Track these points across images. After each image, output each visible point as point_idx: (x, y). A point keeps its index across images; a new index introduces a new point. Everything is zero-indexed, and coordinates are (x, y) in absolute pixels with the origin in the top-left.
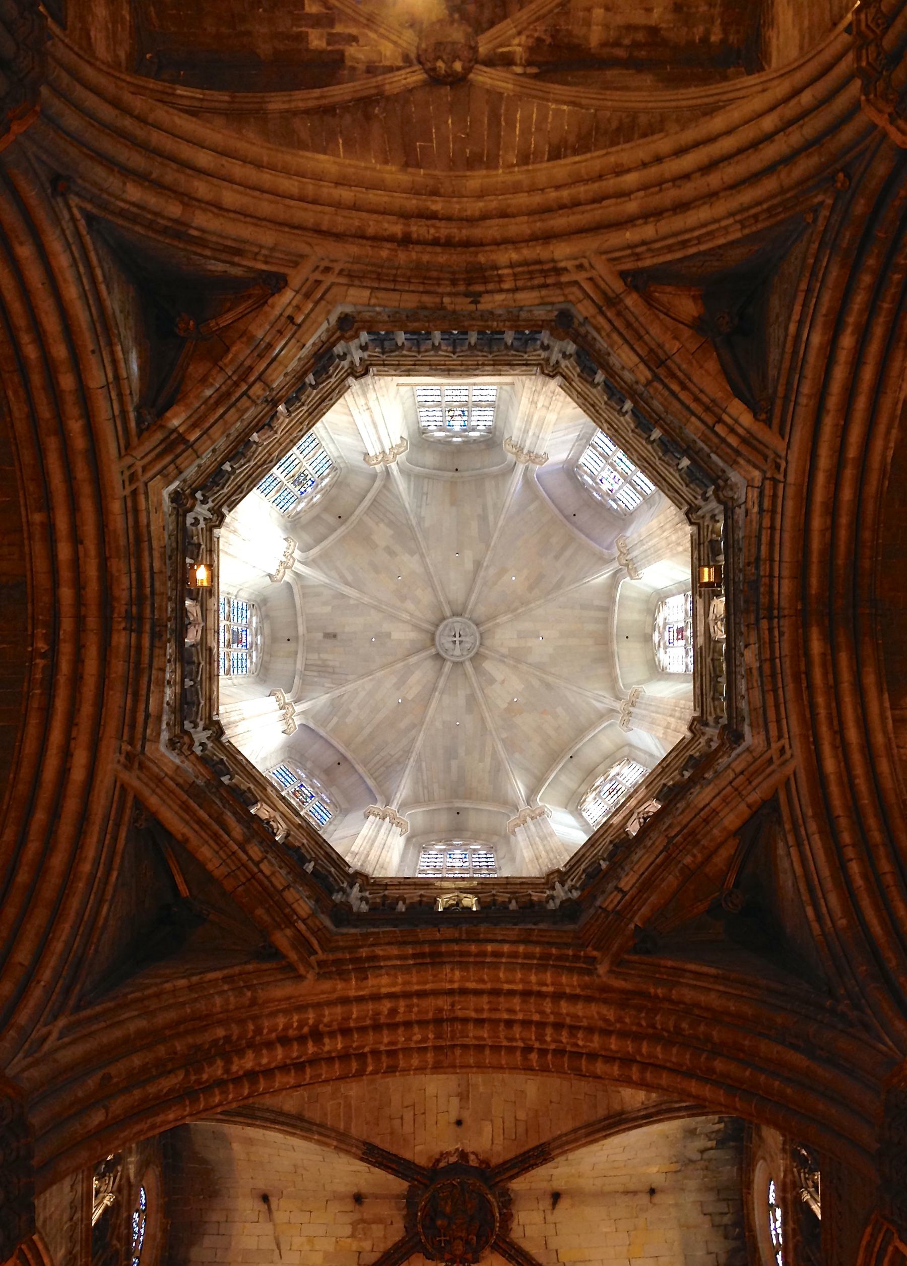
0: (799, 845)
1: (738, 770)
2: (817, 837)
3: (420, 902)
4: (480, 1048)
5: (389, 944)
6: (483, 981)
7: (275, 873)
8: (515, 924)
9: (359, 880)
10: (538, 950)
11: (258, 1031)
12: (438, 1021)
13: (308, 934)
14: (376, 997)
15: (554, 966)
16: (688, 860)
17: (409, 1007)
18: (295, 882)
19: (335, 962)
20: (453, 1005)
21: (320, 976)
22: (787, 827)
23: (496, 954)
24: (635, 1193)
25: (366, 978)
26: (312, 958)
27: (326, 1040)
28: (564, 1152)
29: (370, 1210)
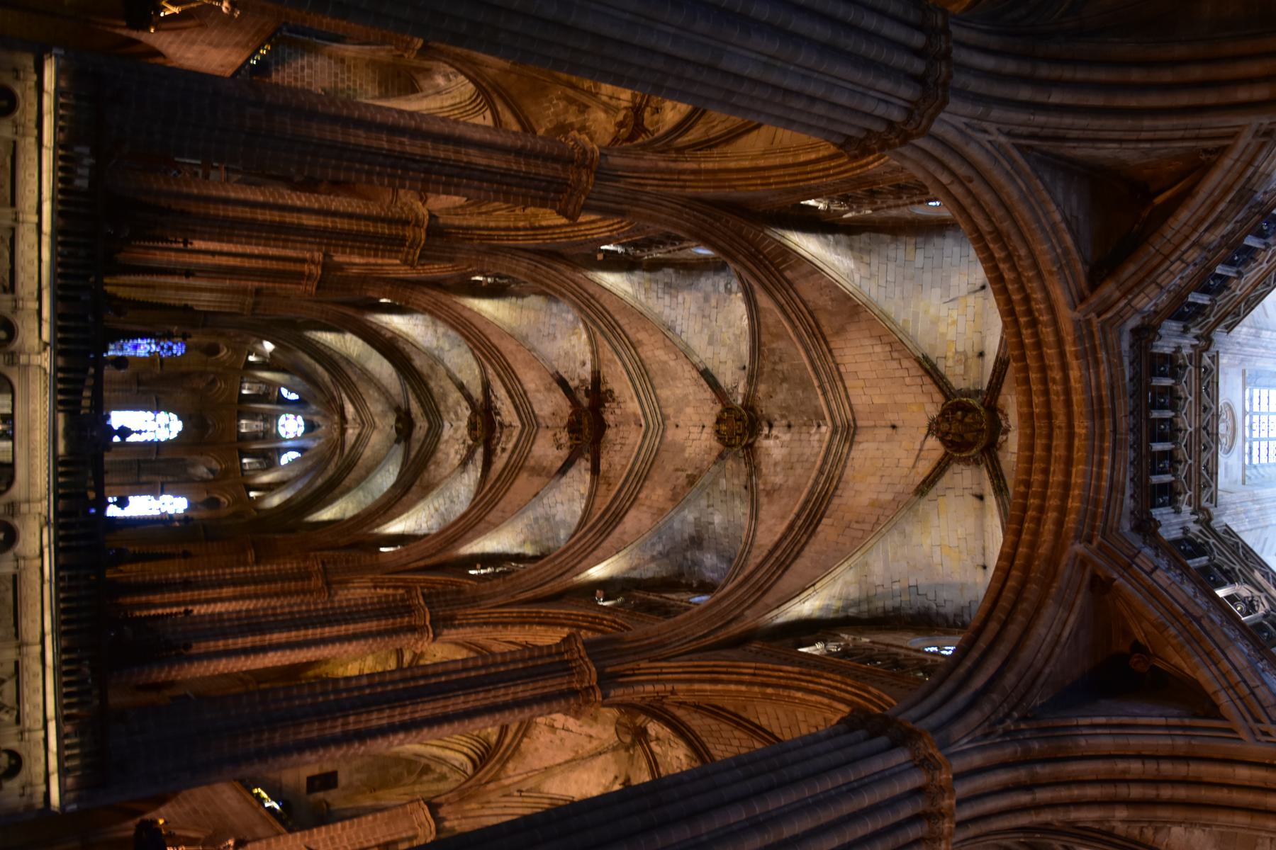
0: (1167, 727)
1: (1257, 691)
2: (1169, 742)
3: (1180, 398)
4: (1031, 448)
5: (1111, 376)
6: (1079, 451)
7: (1176, 275)
8: (1132, 480)
9: (1203, 343)
10: (1104, 497)
11: (1029, 280)
12: (1049, 416)
13: (1115, 310)
14: (1065, 368)
15: (1086, 510)
16: (1172, 631)
17: (1057, 394)
18: (1169, 292)
19: (1092, 335)
20: (1060, 427)
21: (1076, 323)
22: (1187, 722)
23: (1101, 464)
24: (984, 555)
25: (1077, 359)
26: (1093, 315)
27: (1029, 331)
28: (999, 506)
29: (973, 362)
